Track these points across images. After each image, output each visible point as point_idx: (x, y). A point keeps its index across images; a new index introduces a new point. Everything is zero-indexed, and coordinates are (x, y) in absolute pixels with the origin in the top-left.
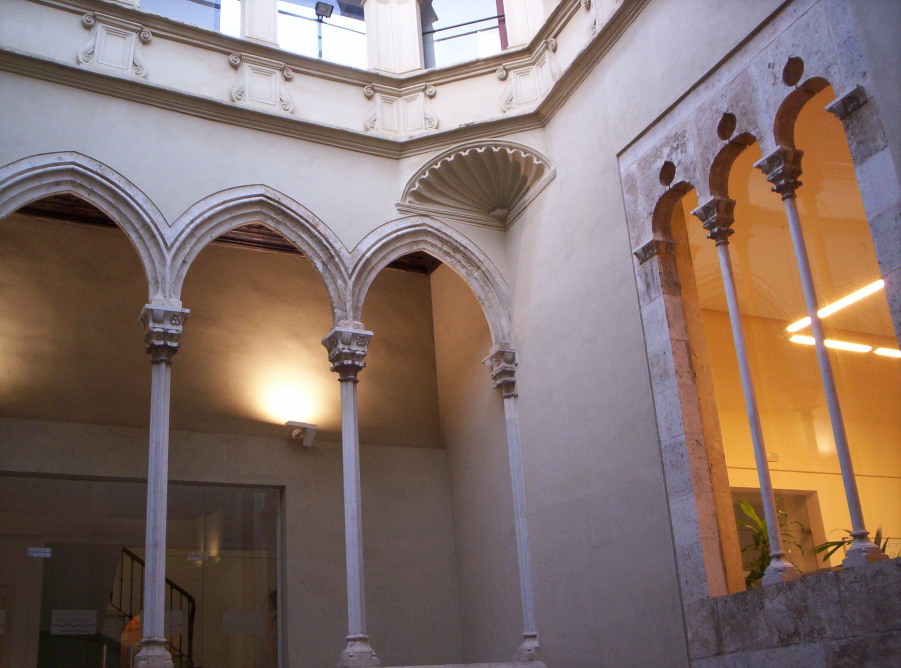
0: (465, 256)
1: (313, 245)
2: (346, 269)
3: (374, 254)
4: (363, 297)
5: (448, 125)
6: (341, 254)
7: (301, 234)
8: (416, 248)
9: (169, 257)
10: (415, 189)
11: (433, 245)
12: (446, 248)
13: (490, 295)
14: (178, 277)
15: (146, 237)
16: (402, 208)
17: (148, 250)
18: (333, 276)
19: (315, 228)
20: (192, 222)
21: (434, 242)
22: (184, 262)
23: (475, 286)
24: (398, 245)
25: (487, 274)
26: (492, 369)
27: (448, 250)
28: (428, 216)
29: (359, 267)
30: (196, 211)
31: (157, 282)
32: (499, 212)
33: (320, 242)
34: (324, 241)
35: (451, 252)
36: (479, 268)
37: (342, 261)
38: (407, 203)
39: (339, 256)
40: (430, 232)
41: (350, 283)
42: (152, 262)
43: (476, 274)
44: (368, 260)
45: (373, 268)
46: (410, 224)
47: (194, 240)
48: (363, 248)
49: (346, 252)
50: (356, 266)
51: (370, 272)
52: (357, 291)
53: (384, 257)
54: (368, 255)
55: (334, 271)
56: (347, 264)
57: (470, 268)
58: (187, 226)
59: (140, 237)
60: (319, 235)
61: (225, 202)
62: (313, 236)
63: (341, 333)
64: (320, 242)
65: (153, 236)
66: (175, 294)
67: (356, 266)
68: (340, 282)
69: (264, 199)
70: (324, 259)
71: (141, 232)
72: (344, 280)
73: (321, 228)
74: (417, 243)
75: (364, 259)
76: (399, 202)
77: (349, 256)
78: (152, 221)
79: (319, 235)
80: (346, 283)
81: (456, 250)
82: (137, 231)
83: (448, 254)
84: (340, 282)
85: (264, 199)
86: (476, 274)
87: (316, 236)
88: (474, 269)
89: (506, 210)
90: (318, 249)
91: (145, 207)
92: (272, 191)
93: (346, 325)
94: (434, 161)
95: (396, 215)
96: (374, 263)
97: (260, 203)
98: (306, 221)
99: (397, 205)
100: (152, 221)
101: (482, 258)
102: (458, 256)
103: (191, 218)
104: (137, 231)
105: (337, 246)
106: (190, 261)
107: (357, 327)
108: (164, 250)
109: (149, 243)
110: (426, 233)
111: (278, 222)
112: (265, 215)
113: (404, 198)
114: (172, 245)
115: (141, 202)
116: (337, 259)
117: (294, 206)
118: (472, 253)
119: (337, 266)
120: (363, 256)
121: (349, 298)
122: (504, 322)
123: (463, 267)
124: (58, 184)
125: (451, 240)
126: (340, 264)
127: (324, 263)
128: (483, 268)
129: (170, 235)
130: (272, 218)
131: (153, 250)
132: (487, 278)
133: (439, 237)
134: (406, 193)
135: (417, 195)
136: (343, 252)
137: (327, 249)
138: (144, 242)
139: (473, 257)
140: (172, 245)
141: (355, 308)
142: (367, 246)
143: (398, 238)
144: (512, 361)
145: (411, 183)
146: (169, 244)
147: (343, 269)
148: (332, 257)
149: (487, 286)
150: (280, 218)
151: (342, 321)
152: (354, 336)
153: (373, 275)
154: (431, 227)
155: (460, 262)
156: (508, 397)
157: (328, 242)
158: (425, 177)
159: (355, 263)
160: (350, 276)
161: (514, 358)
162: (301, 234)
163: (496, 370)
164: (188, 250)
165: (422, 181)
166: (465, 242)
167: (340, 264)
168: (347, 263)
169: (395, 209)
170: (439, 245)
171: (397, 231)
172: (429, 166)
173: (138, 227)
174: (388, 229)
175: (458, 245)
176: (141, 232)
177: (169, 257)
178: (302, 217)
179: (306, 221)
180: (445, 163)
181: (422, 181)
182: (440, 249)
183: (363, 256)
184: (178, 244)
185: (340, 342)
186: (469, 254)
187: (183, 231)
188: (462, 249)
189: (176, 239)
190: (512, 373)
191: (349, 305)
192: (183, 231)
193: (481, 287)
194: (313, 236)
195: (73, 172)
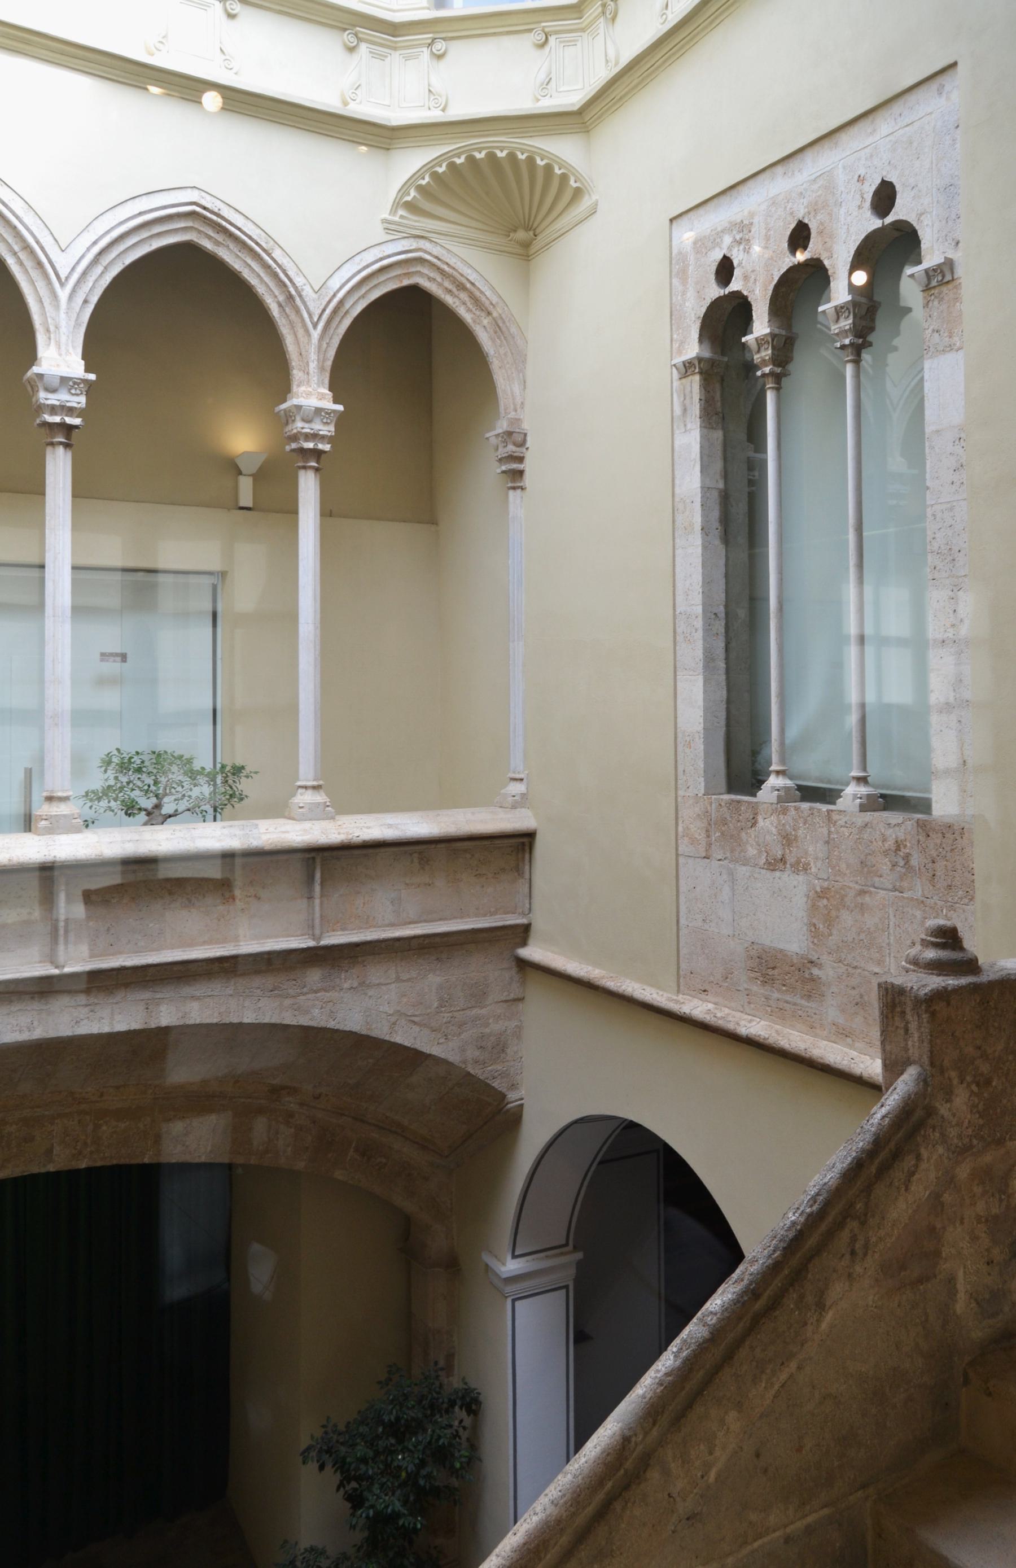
1: (266, 279)
3: (349, 293)
4: (332, 353)
5: (458, 112)
6: (304, 294)
7: (249, 261)
8: (406, 282)
9: (63, 294)
10: (409, 198)
11: (430, 279)
12: (447, 284)
13: (502, 351)
14: (77, 324)
15: (29, 264)
16: (389, 226)
17: (32, 283)
19: (269, 255)
20: (95, 243)
21: (432, 275)
22: (86, 301)
23: (484, 337)
24: (382, 278)
26: (497, 449)
27: (450, 287)
28: (422, 237)
29: (328, 312)
30: (100, 227)
31: (48, 331)
32: (521, 235)
33: (275, 275)
35: (454, 290)
36: (489, 313)
38: (397, 219)
39: (300, 296)
41: (316, 334)
42: (41, 302)
43: (485, 322)
44: (341, 302)
45: (347, 312)
46: (400, 249)
47: (99, 269)
48: (335, 283)
49: (311, 291)
50: (324, 310)
51: (343, 317)
52: (325, 345)
53: (363, 297)
54: (340, 295)
55: (293, 316)
56: (311, 308)
57: (478, 313)
58: (88, 249)
59: (21, 263)
60: (274, 265)
61: (140, 214)
63: (299, 408)
65: (40, 264)
66: (74, 347)
67: (324, 310)
68: (301, 332)
69: (198, 209)
71: (22, 255)
72: (307, 331)
73: (277, 254)
74: (408, 275)
77: (314, 296)
78: (38, 242)
79: (274, 265)
80: (308, 334)
81: (461, 287)
82: (15, 254)
83: (450, 291)
84: (301, 332)
85: (198, 209)
87: (269, 267)
88: (483, 314)
89: (531, 233)
90: (272, 284)
91: (26, 220)
92: (208, 197)
93: (309, 395)
94: (437, 161)
96: (347, 306)
97: (192, 214)
98: (257, 243)
99: (384, 221)
100: (38, 242)
101: (494, 299)
102: (463, 296)
104: (15, 254)
105: (299, 281)
106: (94, 299)
107: (321, 397)
109: (34, 274)
110: (421, 261)
111: (217, 243)
112: (200, 232)
113: (393, 211)
114: (67, 278)
115: (20, 212)
116: (298, 299)
117: (239, 221)
118: (482, 292)
119: (298, 311)
120: (334, 295)
121: (313, 356)
122: (517, 389)
123: (469, 310)
125: (455, 273)
126: (302, 308)
127: (280, 305)
128: (495, 314)
129: (63, 263)
130: (209, 238)
131: (40, 284)
132: (499, 329)
133: (439, 268)
134: (397, 205)
136: (308, 292)
137: (285, 285)
138: (26, 272)
139: (483, 299)
140: (67, 278)
141: (322, 369)
142: (340, 282)
144: (522, 444)
145: (404, 190)
146: (63, 277)
147: (305, 315)
148: (290, 297)
149: (499, 338)
150: (220, 238)
151: (303, 389)
152: (318, 411)
153: (347, 322)
154: (430, 254)
155: (464, 303)
158: (423, 182)
159: (322, 307)
160: (315, 326)
161: (524, 441)
162: (249, 261)
163: (502, 452)
164: (90, 284)
165: (420, 189)
167: (302, 308)
168: (311, 305)
171: (381, 259)
172: (429, 168)
173: (16, 248)
174: (369, 257)
175: (464, 281)
176: (22, 255)
177: (63, 294)
178: (250, 238)
179: (257, 243)
180: (452, 166)
181: (420, 189)
182: (440, 285)
183: (334, 295)
184: (75, 276)
185: (298, 418)
186: (477, 294)
187: (83, 257)
188: (468, 285)
189: (73, 269)
190: (521, 459)
191: (313, 366)
192: (83, 257)
193: (493, 340)
194: (267, 267)
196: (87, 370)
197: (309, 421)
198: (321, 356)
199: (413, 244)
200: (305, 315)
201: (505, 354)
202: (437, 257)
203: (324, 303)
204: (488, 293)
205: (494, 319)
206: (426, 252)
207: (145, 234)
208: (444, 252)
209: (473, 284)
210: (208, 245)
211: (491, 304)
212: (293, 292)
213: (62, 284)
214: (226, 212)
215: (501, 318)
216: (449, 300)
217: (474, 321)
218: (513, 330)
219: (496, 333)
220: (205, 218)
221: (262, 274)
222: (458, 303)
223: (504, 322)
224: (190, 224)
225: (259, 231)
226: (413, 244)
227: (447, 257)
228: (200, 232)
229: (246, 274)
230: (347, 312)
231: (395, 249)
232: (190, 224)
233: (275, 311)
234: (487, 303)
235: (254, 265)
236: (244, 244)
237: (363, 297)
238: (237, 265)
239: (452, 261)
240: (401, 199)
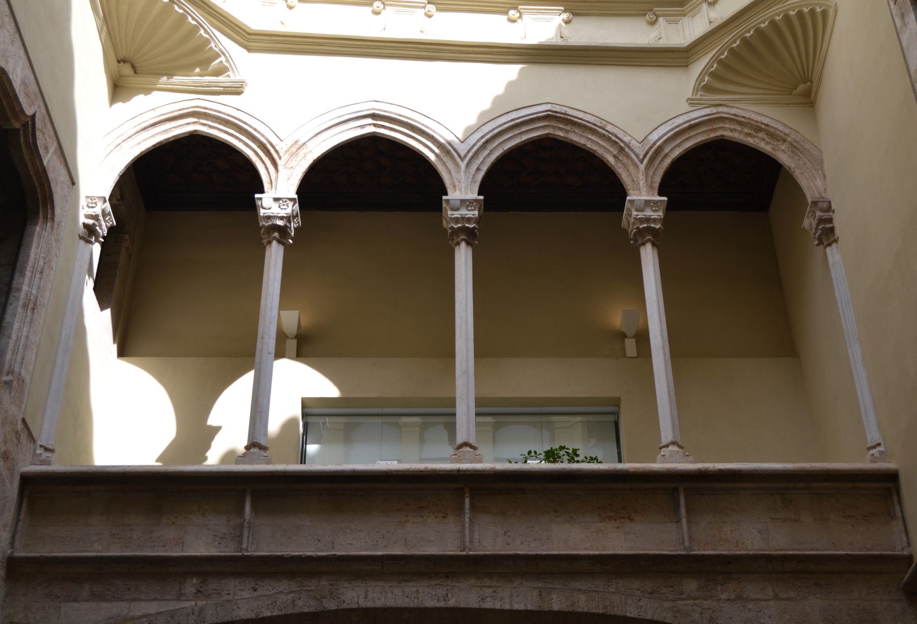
0: (769, 134)
2: (637, 156)
7: (590, 136)
8: (712, 135)
11: (731, 130)
12: (746, 130)
18: (624, 165)
19: (604, 129)
20: (482, 137)
23: (783, 157)
25: (795, 144)
28: (721, 105)
33: (609, 139)
34: (613, 138)
35: (753, 133)
36: (784, 141)
37: (632, 150)
38: (698, 97)
39: (629, 147)
40: (727, 118)
41: (642, 167)
43: (783, 147)
44: (660, 148)
45: (667, 155)
47: (487, 152)
48: (655, 136)
49: (636, 143)
54: (659, 143)
55: (625, 160)
61: (512, 120)
62: (602, 136)
64: (609, 139)
68: (631, 168)
70: (615, 153)
73: (609, 128)
75: (655, 147)
76: (690, 96)
83: (749, 135)
84: (631, 168)
86: (783, 147)
88: (780, 143)
95: (686, 107)
96: (667, 150)
99: (688, 99)
101: (787, 131)
102: (761, 135)
103: (482, 134)
105: (627, 139)
108: (458, 160)
112: (554, 127)
114: (465, 156)
116: (627, 149)
117: (581, 115)
119: (628, 156)
123: (768, 143)
124: (362, 127)
127: (615, 156)
128: (789, 139)
130: (561, 129)
132: (795, 148)
134: (696, 90)
135: (707, 89)
136: (634, 143)
137: (616, 143)
139: (777, 132)
140: (465, 156)
143: (691, 127)
146: (462, 155)
147: (633, 156)
149: (797, 155)
150: (568, 128)
152: (647, 202)
155: (763, 139)
156: (830, 245)
157: (617, 138)
160: (642, 162)
162: (590, 136)
165: (712, 75)
166: (766, 121)
168: (637, 151)
169: (686, 105)
170: (739, 128)
178: (589, 122)
181: (712, 75)
182: (740, 132)
183: (654, 144)
184: (471, 154)
185: (633, 210)
189: (469, 151)
191: (642, 183)
194: (602, 136)
195: (373, 116)
196: (479, 194)
197: (642, 211)
198: (649, 180)
199: (714, 110)
200: (633, 156)
201: (804, 164)
202: (734, 115)
203: (647, 148)
204: (781, 128)
205: (790, 143)
206: (724, 113)
207: (516, 132)
208: (740, 111)
209: (767, 125)
210: (561, 134)
211: (785, 134)
212: (622, 145)
213: (462, 160)
214: (570, 112)
215: (796, 141)
216: (750, 141)
217: (774, 149)
218: (807, 146)
219: (793, 152)
220: (556, 117)
221: (600, 142)
222: (758, 141)
223: (798, 143)
224: (547, 123)
225: (594, 118)
226: (714, 110)
227: (742, 113)
228: (554, 127)
229: (589, 145)
230: (667, 155)
231: (698, 114)
232: (547, 123)
233: (611, 160)
234: (782, 135)
235: (593, 138)
236: (585, 126)
237: (679, 145)
238: (582, 141)
239: (747, 115)
240: (699, 84)
